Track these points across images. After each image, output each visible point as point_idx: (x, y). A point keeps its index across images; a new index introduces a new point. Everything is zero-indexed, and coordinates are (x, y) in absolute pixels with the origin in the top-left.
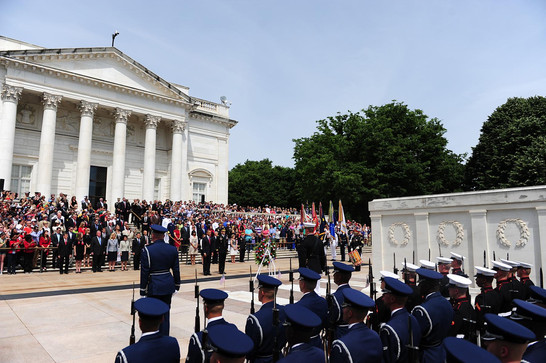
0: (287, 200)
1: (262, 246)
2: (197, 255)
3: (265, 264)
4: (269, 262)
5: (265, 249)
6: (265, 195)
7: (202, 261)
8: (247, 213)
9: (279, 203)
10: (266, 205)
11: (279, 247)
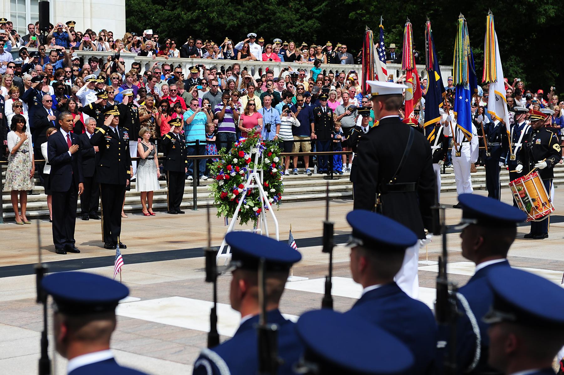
0: (317, 18)
1: (235, 160)
2: (31, 192)
4: (260, 208)
5: (245, 170)
7: (49, 212)
8: (189, 60)
11: (291, 166)
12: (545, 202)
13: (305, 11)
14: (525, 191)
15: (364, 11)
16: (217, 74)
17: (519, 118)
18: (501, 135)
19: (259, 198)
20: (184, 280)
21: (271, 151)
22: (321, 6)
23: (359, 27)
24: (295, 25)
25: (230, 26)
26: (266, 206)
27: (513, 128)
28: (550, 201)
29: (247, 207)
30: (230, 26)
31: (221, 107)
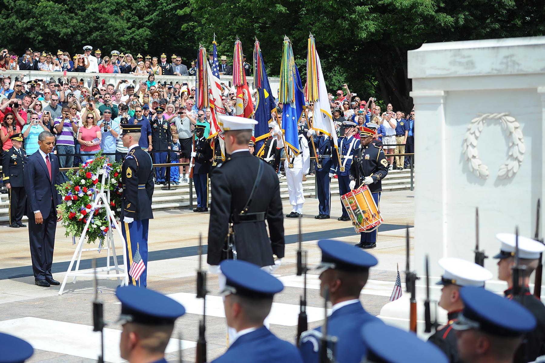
0: (148, 27)
1: (83, 182)
3: (93, 235)
4: (107, 227)
5: (92, 190)
6: (80, 12)
9: (122, 38)
10: (85, 48)
12: (375, 214)
13: (136, 20)
15: (196, 23)
16: (56, 86)
17: (348, 131)
18: (331, 147)
19: (106, 218)
20: (34, 299)
21: (117, 172)
22: (153, 16)
23: (189, 36)
24: (127, 33)
25: (63, 33)
26: (113, 225)
27: (342, 141)
28: (379, 213)
29: (95, 226)
30: (63, 33)
31: (60, 120)
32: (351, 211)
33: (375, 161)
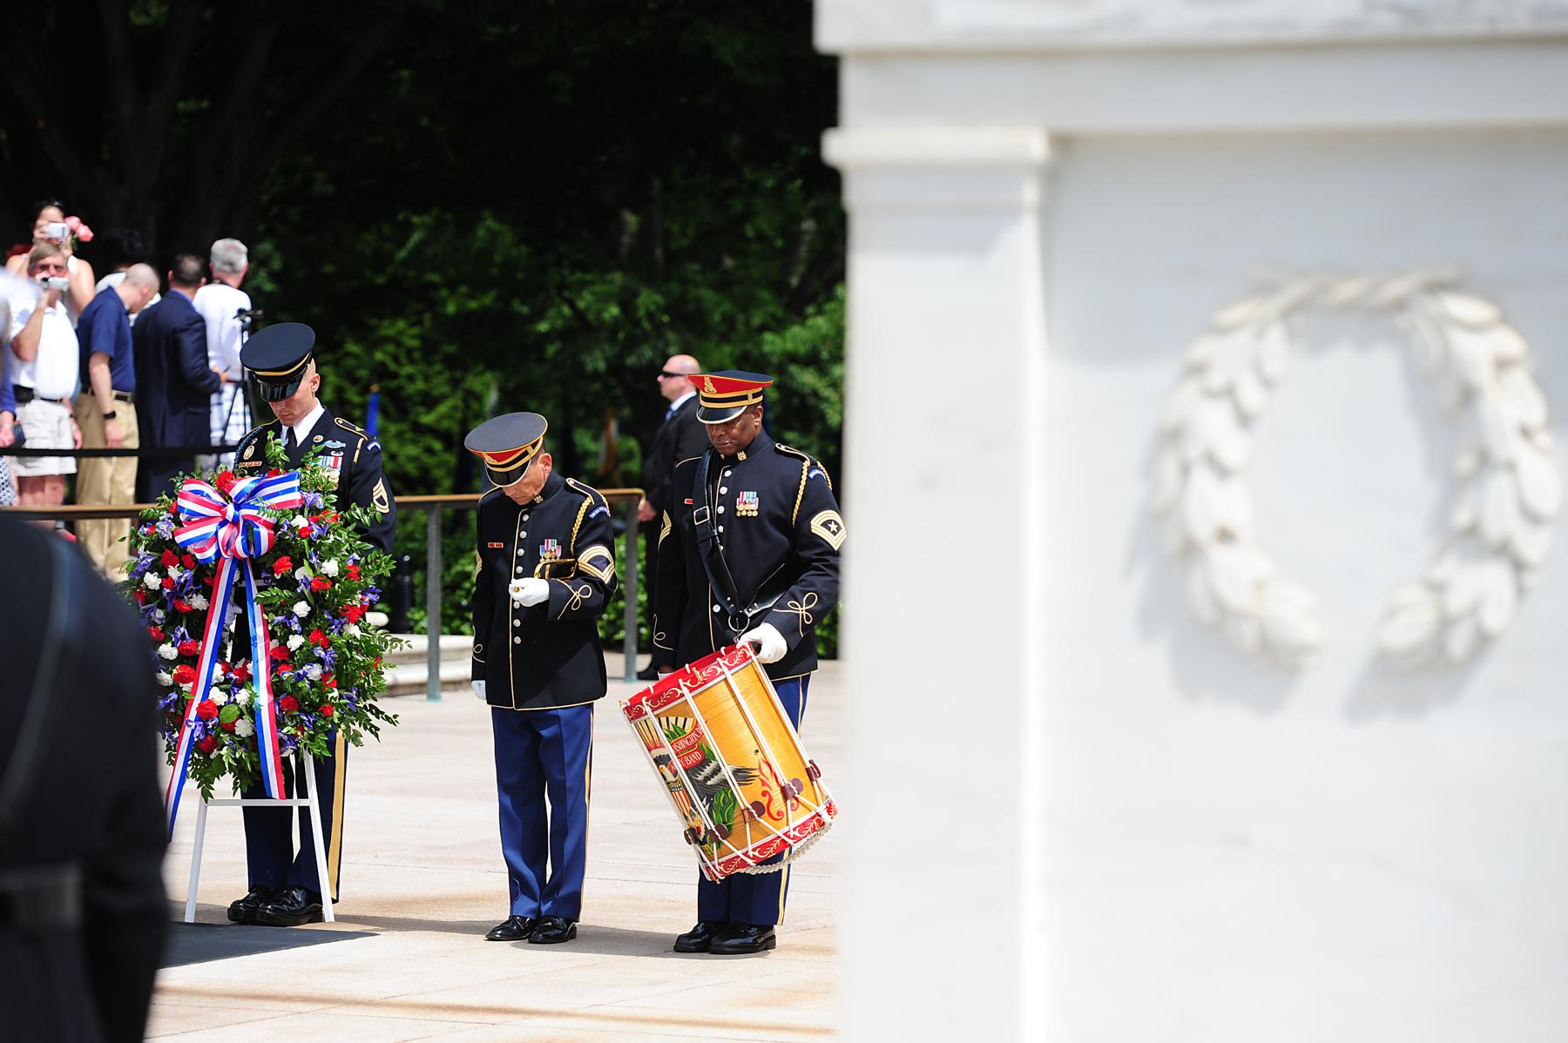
14: (701, 736)
32: (675, 773)
33: (782, 523)
